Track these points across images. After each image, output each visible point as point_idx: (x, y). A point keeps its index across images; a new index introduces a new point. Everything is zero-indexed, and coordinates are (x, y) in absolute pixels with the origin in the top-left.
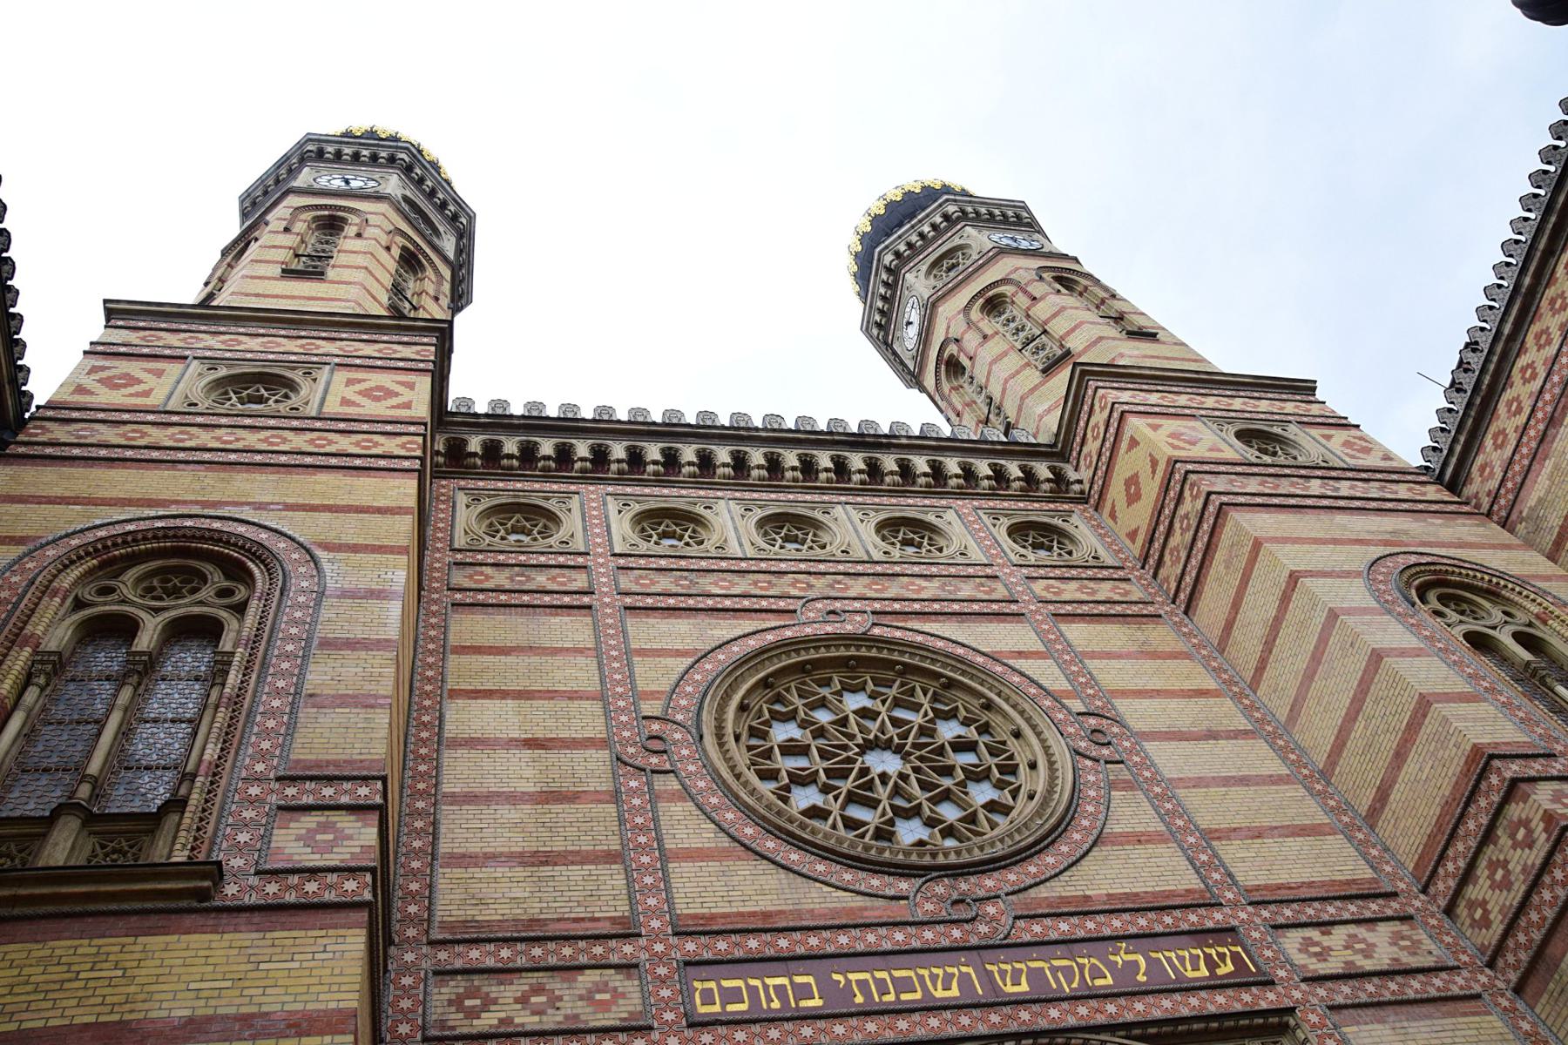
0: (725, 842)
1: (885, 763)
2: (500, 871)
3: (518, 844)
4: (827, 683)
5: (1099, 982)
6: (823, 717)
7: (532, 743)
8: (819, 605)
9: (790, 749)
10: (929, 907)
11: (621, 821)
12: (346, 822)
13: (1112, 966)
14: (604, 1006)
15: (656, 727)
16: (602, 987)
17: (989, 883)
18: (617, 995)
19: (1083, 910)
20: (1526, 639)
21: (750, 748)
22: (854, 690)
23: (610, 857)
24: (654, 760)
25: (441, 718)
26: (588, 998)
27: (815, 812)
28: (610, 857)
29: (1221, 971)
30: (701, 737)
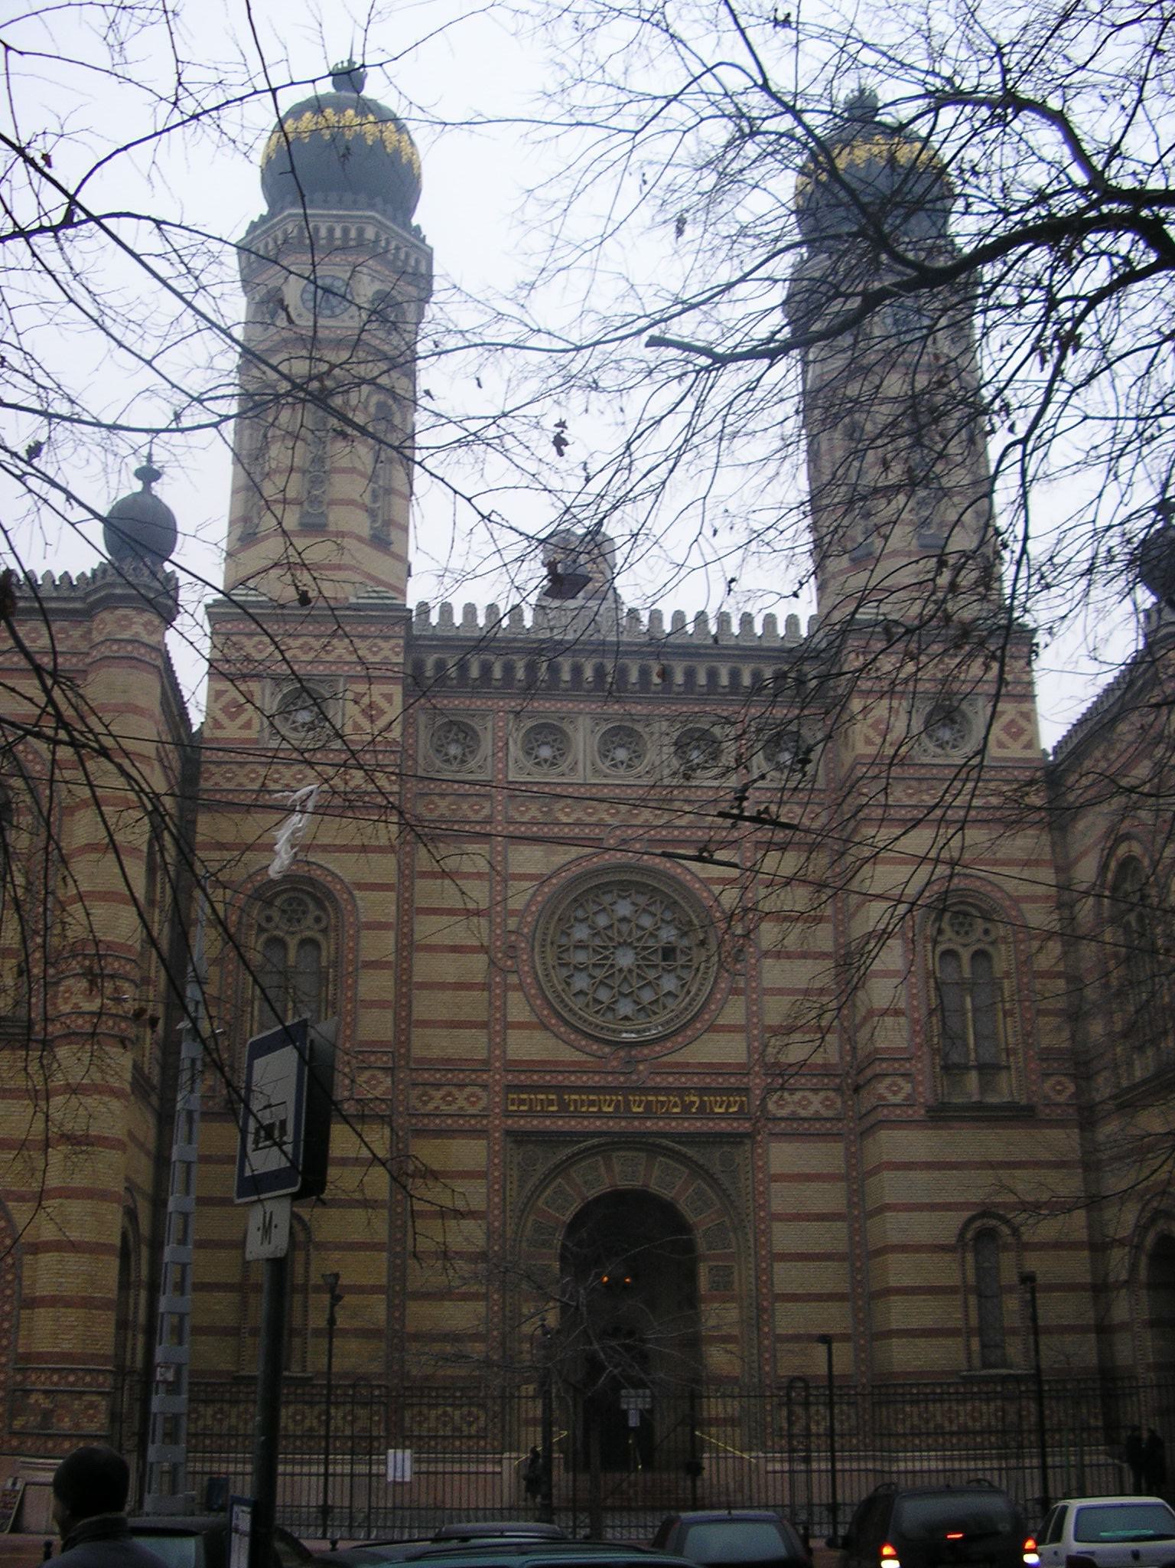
0: (535, 1020)
1: (626, 959)
2: (438, 1031)
3: (444, 1014)
4: (611, 892)
5: (675, 1110)
6: (602, 921)
7: (455, 949)
8: (618, 832)
9: (581, 946)
10: (615, 1063)
11: (490, 1004)
12: (380, 1075)
13: (683, 1101)
14: (473, 1104)
15: (513, 938)
16: (473, 1095)
17: (646, 1051)
18: (479, 1099)
19: (682, 1068)
20: (980, 955)
21: (560, 947)
22: (624, 898)
23: (485, 1025)
24: (509, 963)
25: (412, 930)
26: (467, 1099)
27: (581, 992)
28: (485, 1025)
29: (731, 1110)
30: (533, 949)
